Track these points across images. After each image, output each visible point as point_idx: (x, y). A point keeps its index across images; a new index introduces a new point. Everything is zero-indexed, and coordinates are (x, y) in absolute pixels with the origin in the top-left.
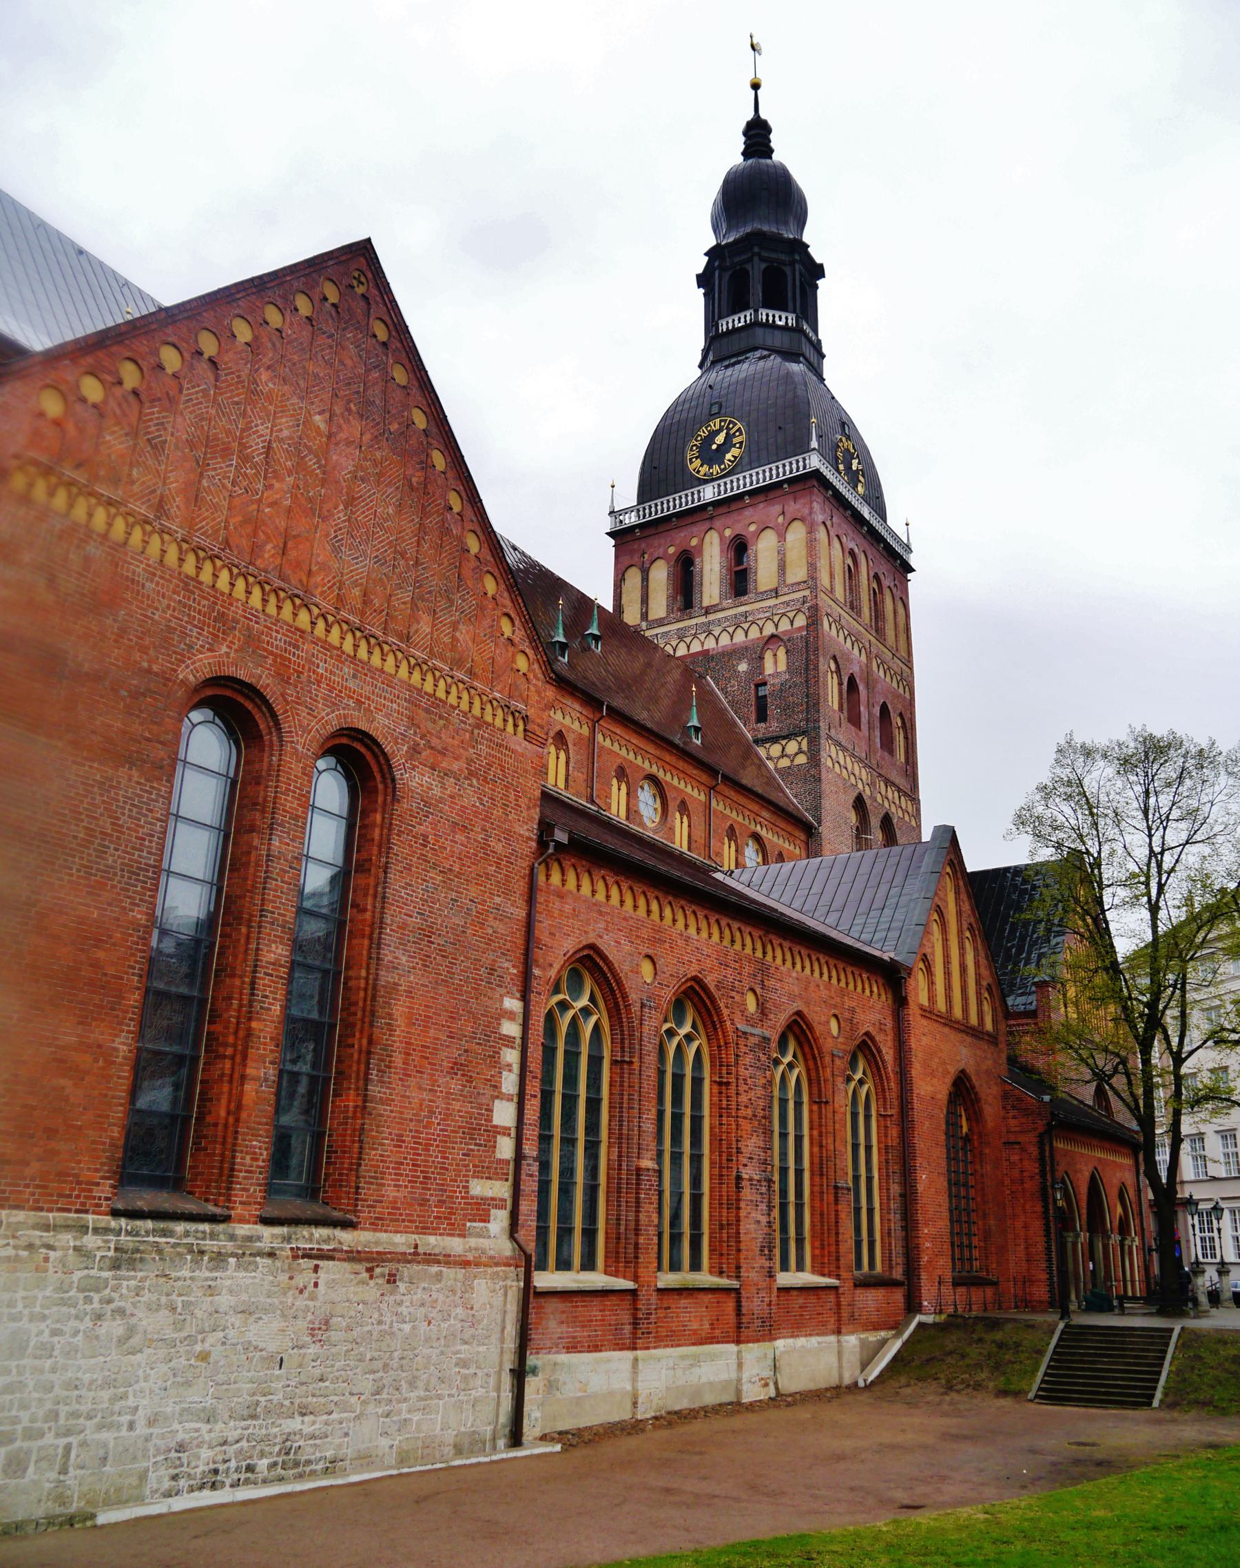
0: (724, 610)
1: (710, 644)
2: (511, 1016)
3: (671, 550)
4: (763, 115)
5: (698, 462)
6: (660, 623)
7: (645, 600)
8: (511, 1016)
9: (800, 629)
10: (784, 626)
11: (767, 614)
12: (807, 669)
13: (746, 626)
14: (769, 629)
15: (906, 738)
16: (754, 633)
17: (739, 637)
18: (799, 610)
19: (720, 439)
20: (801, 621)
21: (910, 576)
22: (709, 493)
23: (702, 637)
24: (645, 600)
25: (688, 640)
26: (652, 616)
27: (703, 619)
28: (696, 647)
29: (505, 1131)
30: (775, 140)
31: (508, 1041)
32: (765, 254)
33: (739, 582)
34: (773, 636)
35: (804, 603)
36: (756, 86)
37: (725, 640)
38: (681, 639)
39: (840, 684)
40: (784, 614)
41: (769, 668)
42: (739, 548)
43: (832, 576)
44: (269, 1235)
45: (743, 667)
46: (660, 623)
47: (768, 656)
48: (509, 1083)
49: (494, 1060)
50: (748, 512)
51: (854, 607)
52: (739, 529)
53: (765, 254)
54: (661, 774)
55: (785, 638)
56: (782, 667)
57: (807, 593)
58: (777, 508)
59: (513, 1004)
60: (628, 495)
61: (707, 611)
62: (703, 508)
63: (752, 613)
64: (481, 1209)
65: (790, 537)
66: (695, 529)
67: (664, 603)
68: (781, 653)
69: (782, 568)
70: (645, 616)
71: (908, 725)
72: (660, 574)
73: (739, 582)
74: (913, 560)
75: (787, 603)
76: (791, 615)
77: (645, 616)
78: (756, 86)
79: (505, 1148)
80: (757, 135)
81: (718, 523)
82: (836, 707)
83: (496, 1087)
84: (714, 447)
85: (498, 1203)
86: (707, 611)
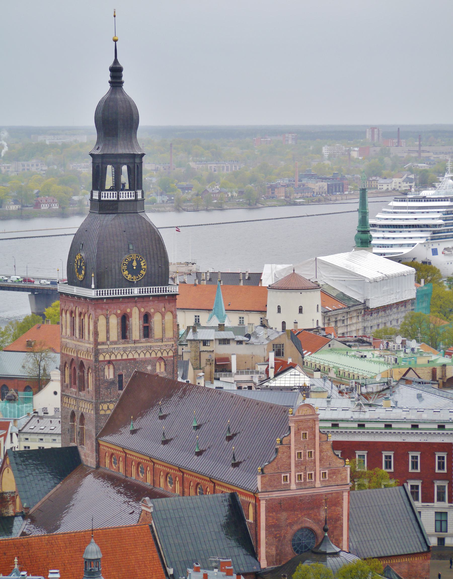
0: (141, 343)
1: (136, 356)
3: (119, 312)
5: (126, 273)
6: (115, 343)
7: (108, 332)
9: (171, 357)
10: (165, 354)
11: (159, 349)
12: (173, 373)
13: (150, 351)
14: (159, 355)
16: (153, 355)
17: (148, 356)
18: (171, 349)
19: (135, 264)
20: (171, 354)
22: (136, 291)
23: (133, 352)
24: (108, 332)
25: (128, 353)
26: (111, 339)
27: (133, 345)
28: (130, 357)
33: (147, 332)
34: (160, 357)
35: (173, 346)
36: (115, 41)
37: (142, 356)
38: (125, 352)
40: (165, 350)
41: (158, 371)
42: (146, 318)
45: (149, 368)
46: (115, 343)
47: (158, 364)
50: (151, 303)
52: (147, 310)
55: (165, 359)
56: (163, 370)
57: (173, 343)
58: (162, 305)
61: (135, 342)
62: (134, 297)
63: (153, 347)
65: (166, 317)
66: (129, 305)
67: (116, 334)
68: (163, 364)
69: (164, 330)
70: (108, 339)
72: (114, 321)
73: (147, 332)
75: (166, 345)
76: (168, 350)
77: (108, 339)
78: (115, 41)
80: (116, 72)
81: (139, 305)
84: (135, 268)
86: (135, 342)
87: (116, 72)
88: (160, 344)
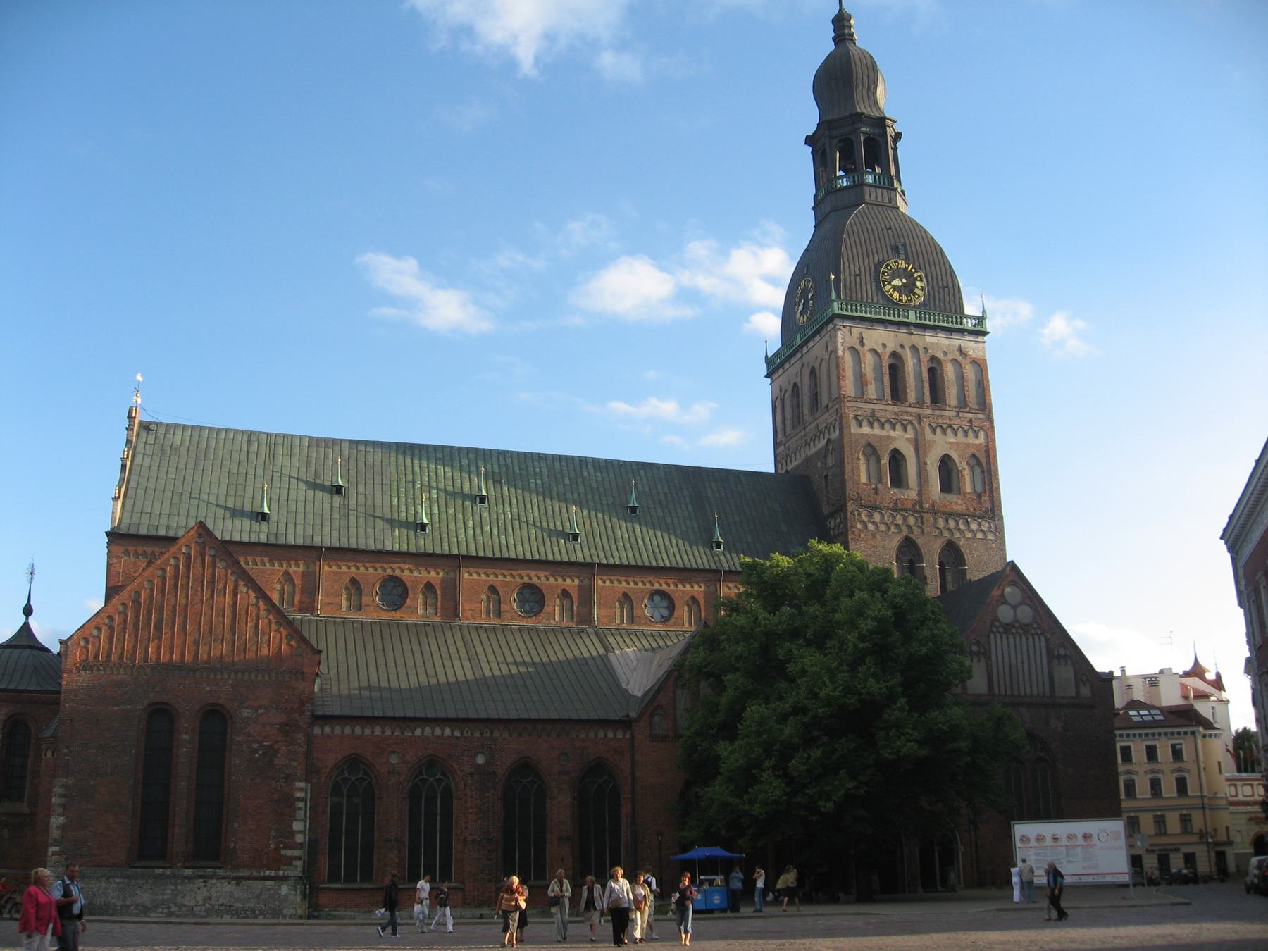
2: (301, 790)
4: (846, 8)
8: (301, 790)
15: (983, 472)
21: (986, 338)
29: (300, 832)
30: (857, 27)
32: (835, 133)
44: (188, 872)
51: (898, 393)
53: (835, 133)
54: (665, 587)
59: (302, 784)
64: (289, 861)
71: (983, 460)
74: (988, 326)
85: (299, 858)
87: (841, 23)
88: (827, 415)
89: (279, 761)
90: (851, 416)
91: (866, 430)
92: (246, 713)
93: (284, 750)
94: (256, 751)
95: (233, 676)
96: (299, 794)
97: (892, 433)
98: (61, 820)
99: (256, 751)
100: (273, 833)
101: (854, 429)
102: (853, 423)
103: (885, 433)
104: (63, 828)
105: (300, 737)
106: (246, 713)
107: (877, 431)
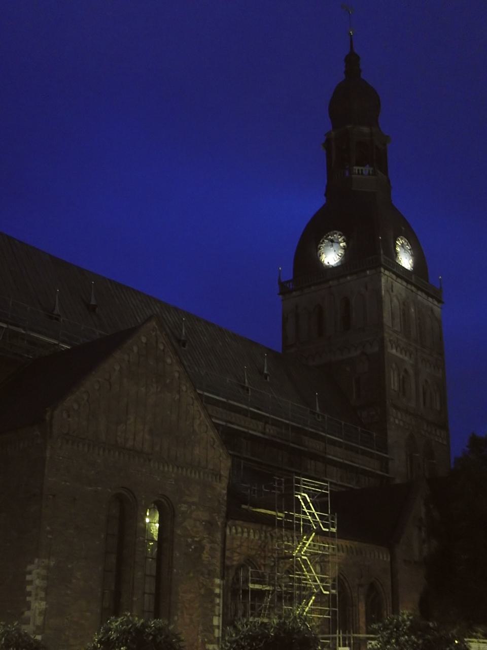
4: (356, 51)
31: (218, 596)
39: (399, 375)
43: (393, 319)
48: (219, 609)
49: (212, 601)
59: (218, 581)
60: (288, 275)
79: (217, 633)
80: (352, 60)
82: (396, 389)
83: (214, 611)
89: (205, 556)
90: (388, 339)
91: (394, 351)
92: (184, 508)
93: (208, 546)
94: (189, 546)
95: (175, 470)
96: (217, 591)
97: (406, 358)
98: (43, 605)
99: (189, 546)
100: (201, 628)
101: (389, 350)
102: (389, 344)
103: (401, 356)
104: (44, 613)
105: (219, 536)
106: (184, 508)
107: (398, 355)
